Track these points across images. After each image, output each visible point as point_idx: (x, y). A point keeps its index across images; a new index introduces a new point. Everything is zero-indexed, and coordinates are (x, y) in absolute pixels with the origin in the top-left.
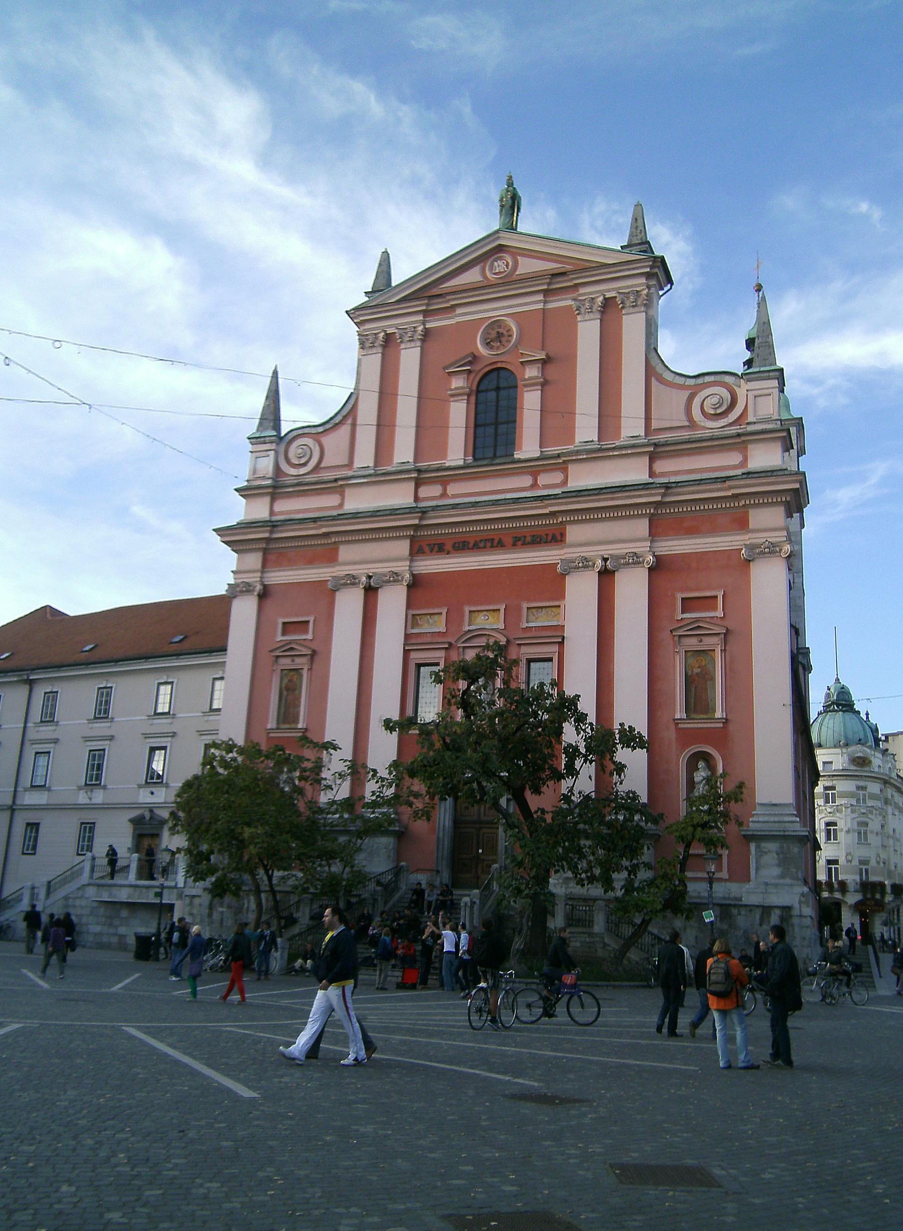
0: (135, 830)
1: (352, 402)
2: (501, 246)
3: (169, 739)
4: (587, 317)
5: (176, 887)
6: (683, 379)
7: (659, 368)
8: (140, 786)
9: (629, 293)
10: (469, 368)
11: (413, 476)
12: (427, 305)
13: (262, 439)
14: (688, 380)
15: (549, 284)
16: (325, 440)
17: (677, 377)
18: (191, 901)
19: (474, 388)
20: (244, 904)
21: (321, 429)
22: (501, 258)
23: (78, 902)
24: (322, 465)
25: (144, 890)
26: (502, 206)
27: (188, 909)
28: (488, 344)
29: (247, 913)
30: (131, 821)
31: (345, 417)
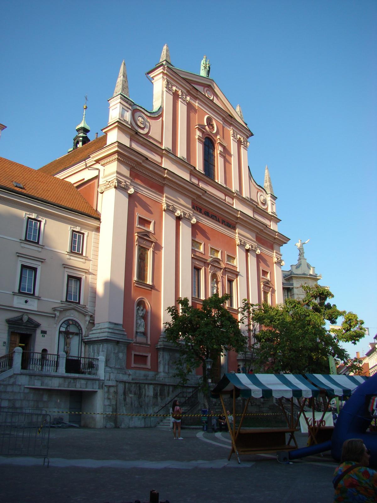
0: (10, 328)
2: (210, 85)
3: (40, 263)
5: (99, 380)
8: (14, 294)
10: (205, 131)
11: (192, 169)
13: (127, 100)
17: (254, 182)
18: (109, 390)
20: (143, 392)
21: (149, 115)
23: (9, 389)
25: (72, 381)
27: (106, 395)
29: (145, 397)
30: (9, 321)
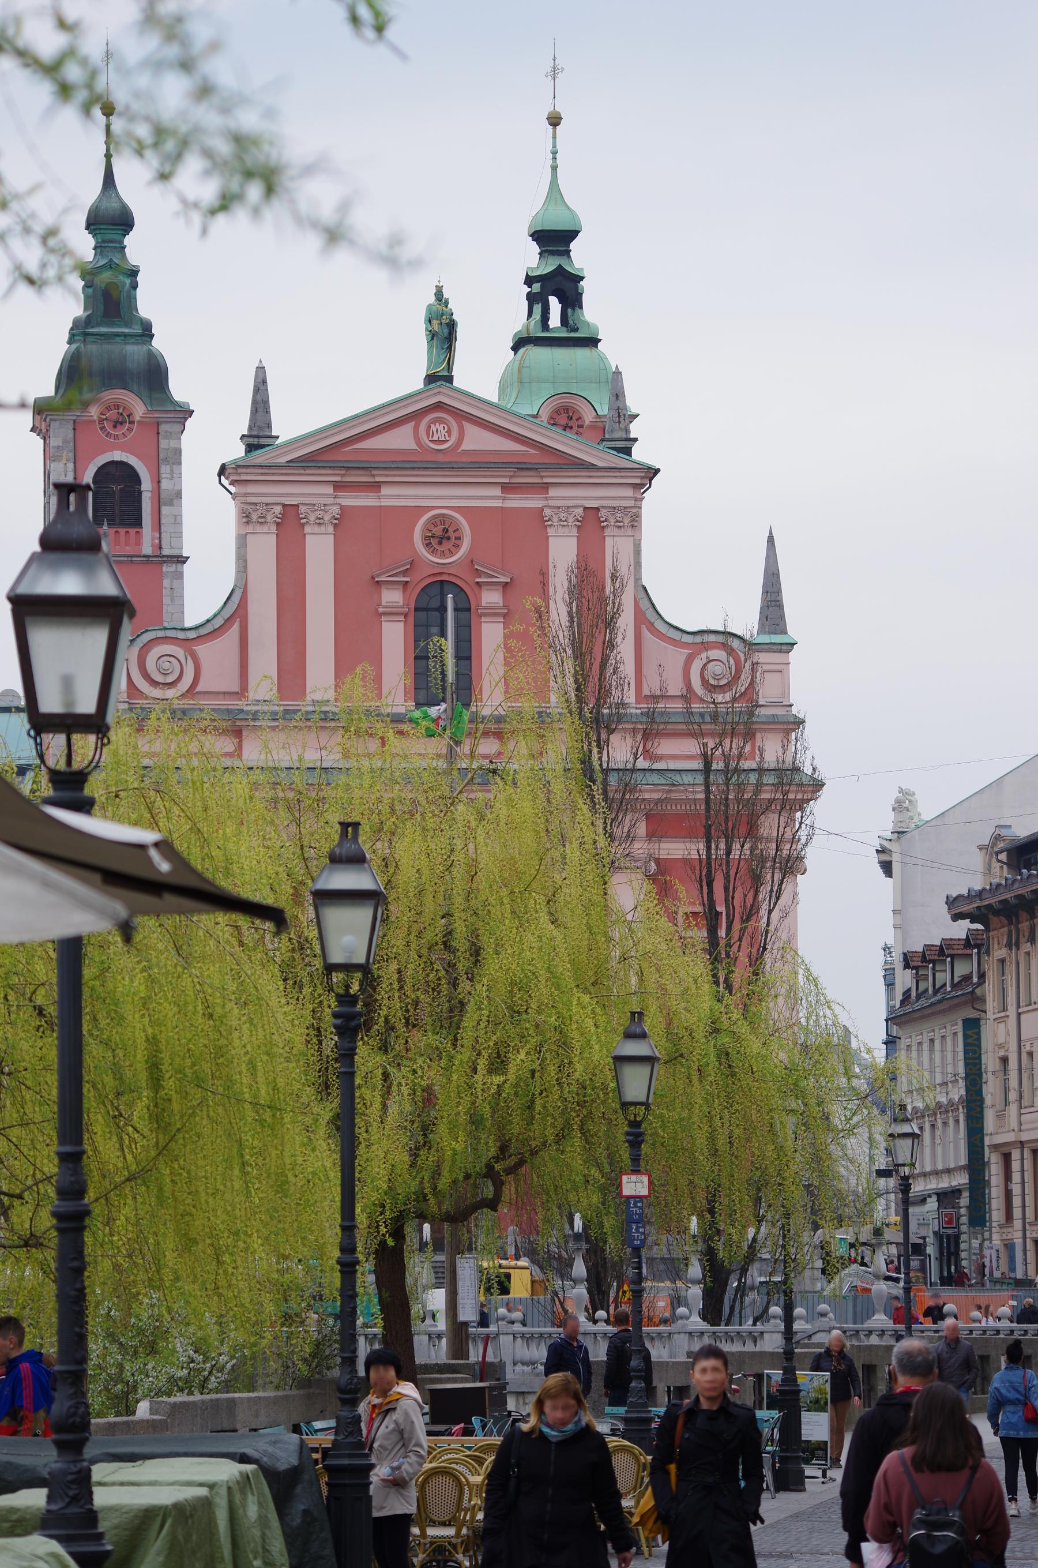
1: (236, 599)
4: (561, 531)
6: (679, 633)
7: (650, 614)
9: (614, 508)
12: (343, 475)
14: (685, 635)
15: (511, 477)
16: (200, 650)
17: (672, 629)
19: (413, 606)
21: (192, 635)
22: (440, 421)
24: (198, 689)
26: (432, 335)
28: (428, 545)
31: (228, 622)
